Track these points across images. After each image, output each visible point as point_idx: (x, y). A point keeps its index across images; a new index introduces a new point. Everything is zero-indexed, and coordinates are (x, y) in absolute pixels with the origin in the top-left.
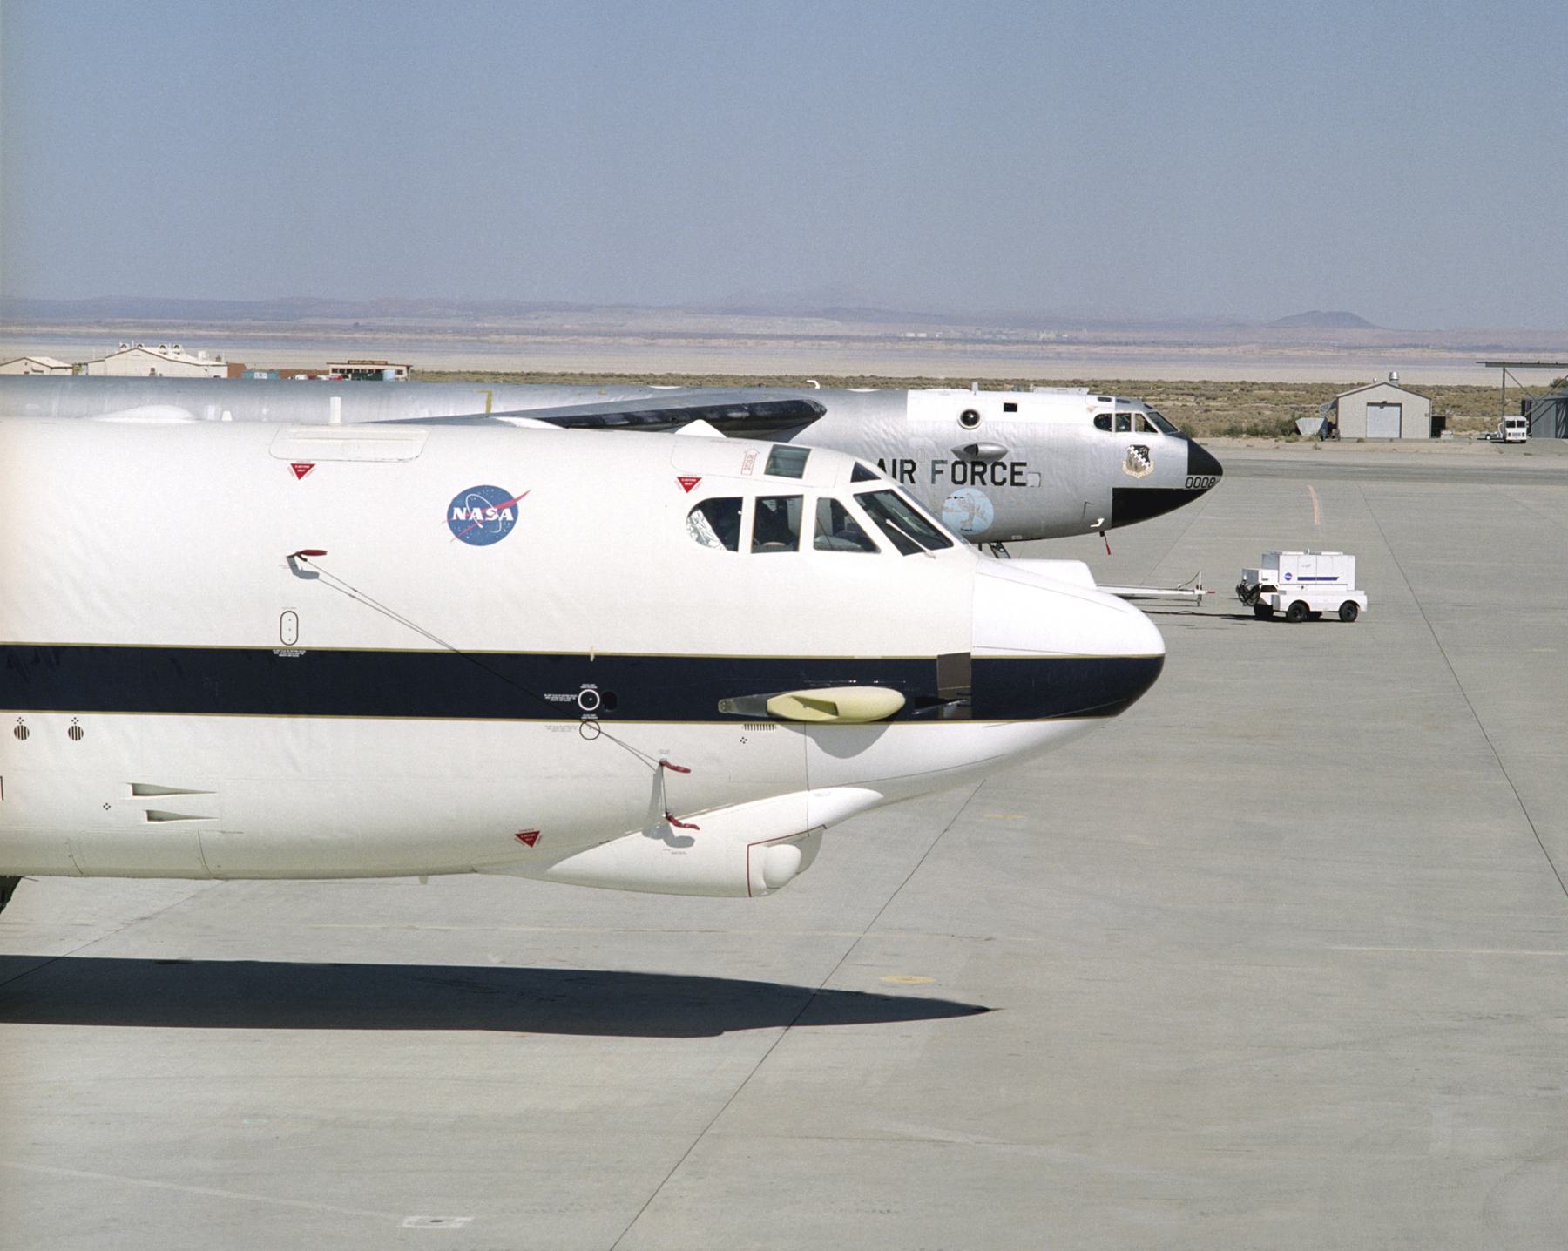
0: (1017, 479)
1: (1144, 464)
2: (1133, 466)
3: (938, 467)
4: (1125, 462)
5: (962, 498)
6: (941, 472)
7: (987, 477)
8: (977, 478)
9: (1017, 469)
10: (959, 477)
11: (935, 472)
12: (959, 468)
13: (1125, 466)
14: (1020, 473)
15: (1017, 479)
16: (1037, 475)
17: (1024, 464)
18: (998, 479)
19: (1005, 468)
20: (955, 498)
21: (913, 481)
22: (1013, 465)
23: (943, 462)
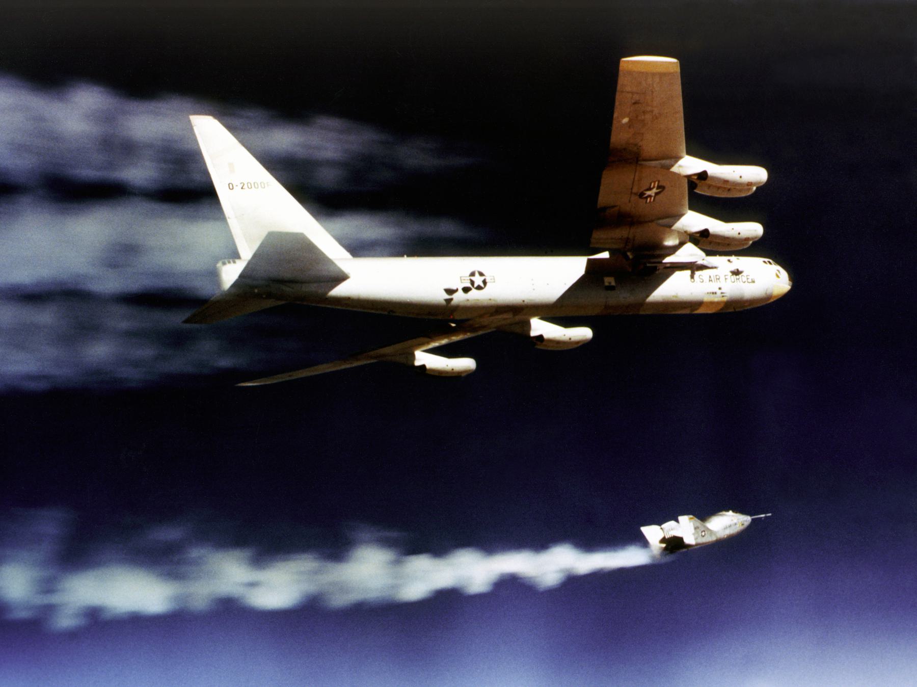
3: (726, 277)
7: (740, 279)
21: (720, 282)
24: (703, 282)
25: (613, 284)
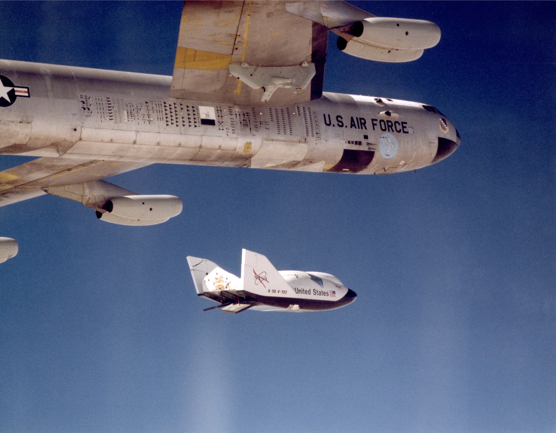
0: (405, 130)
1: (446, 127)
2: (443, 127)
3: (375, 122)
4: (440, 125)
5: (386, 138)
6: (376, 125)
7: (394, 127)
8: (390, 128)
9: (404, 125)
10: (383, 128)
11: (374, 125)
12: (382, 123)
13: (440, 127)
14: (405, 127)
15: (405, 130)
16: (412, 129)
17: (406, 123)
18: (398, 130)
19: (399, 124)
20: (383, 137)
21: (366, 128)
22: (403, 123)
23: (376, 120)
24: (342, 126)
25: (212, 116)
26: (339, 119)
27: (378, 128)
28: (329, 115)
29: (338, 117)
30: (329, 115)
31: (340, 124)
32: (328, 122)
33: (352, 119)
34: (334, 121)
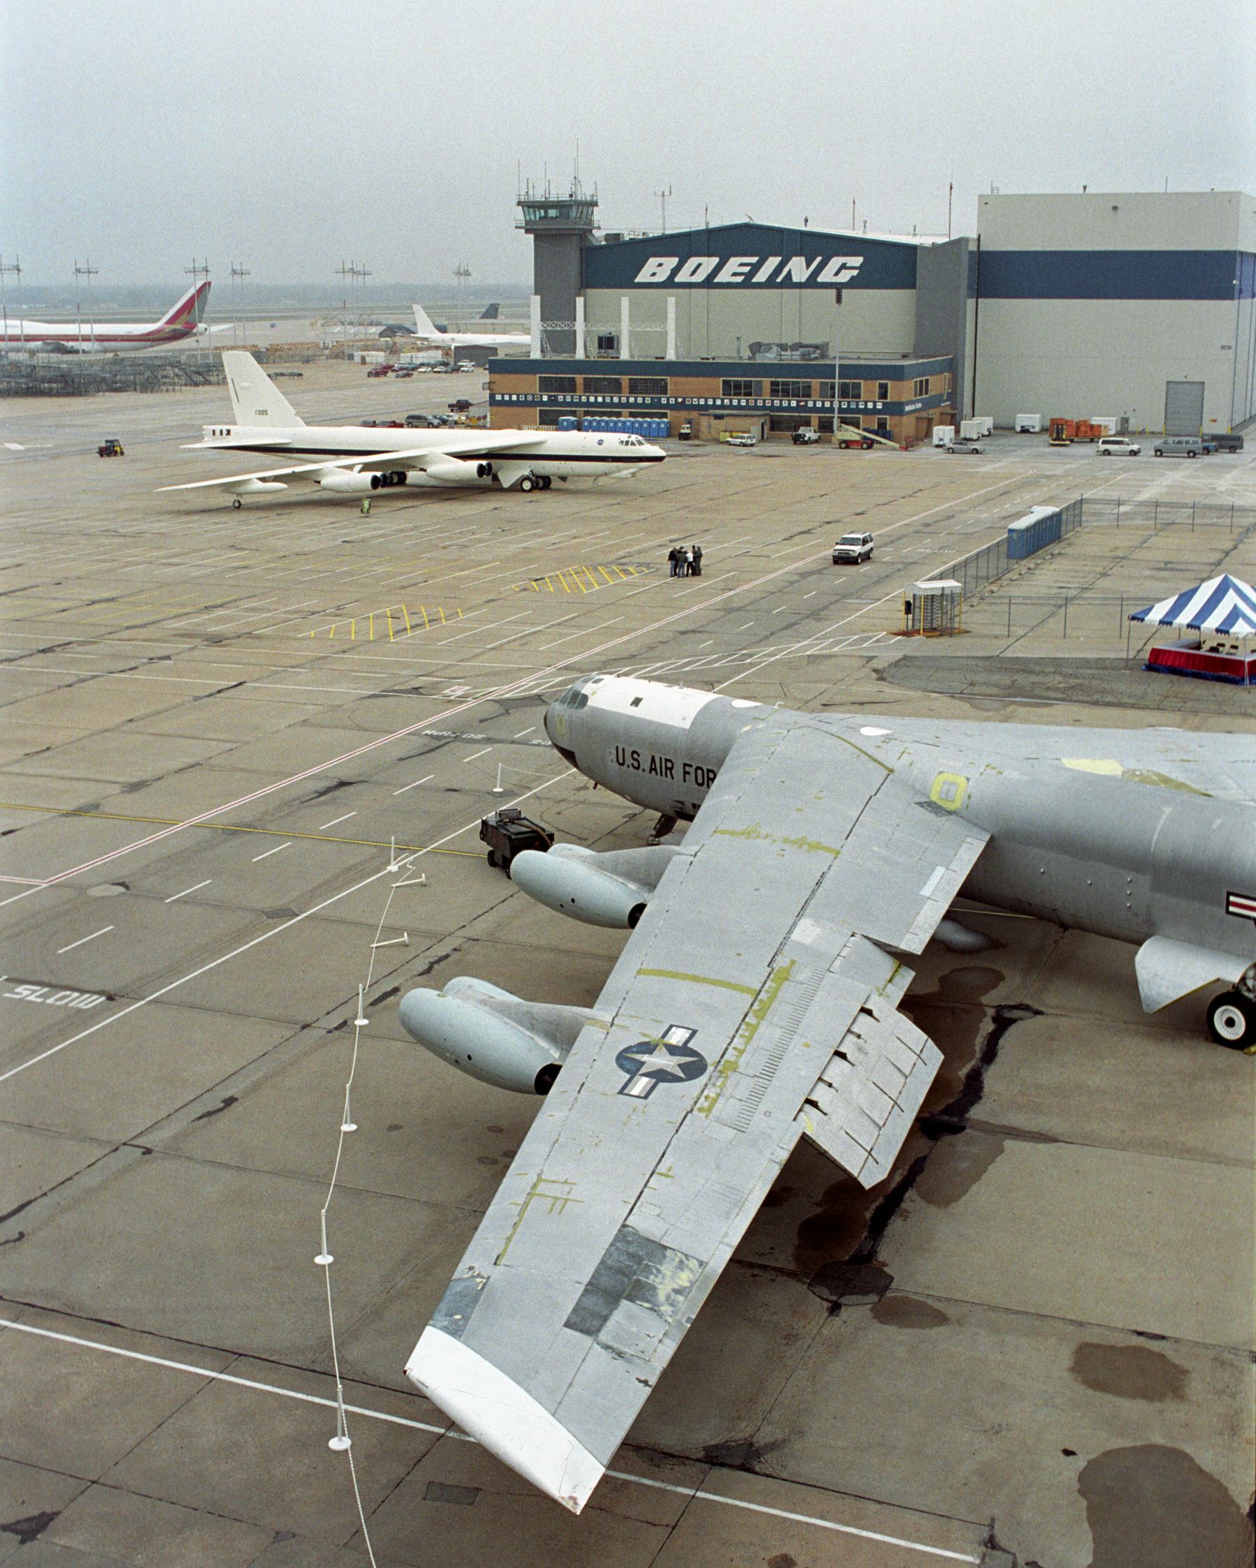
6: (689, 773)
10: (700, 781)
11: (686, 773)
12: (699, 772)
23: (690, 766)
24: (638, 768)
26: (635, 756)
27: (691, 778)
28: (623, 750)
29: (634, 752)
30: (623, 750)
31: (636, 764)
32: (621, 761)
33: (653, 760)
34: (629, 761)
